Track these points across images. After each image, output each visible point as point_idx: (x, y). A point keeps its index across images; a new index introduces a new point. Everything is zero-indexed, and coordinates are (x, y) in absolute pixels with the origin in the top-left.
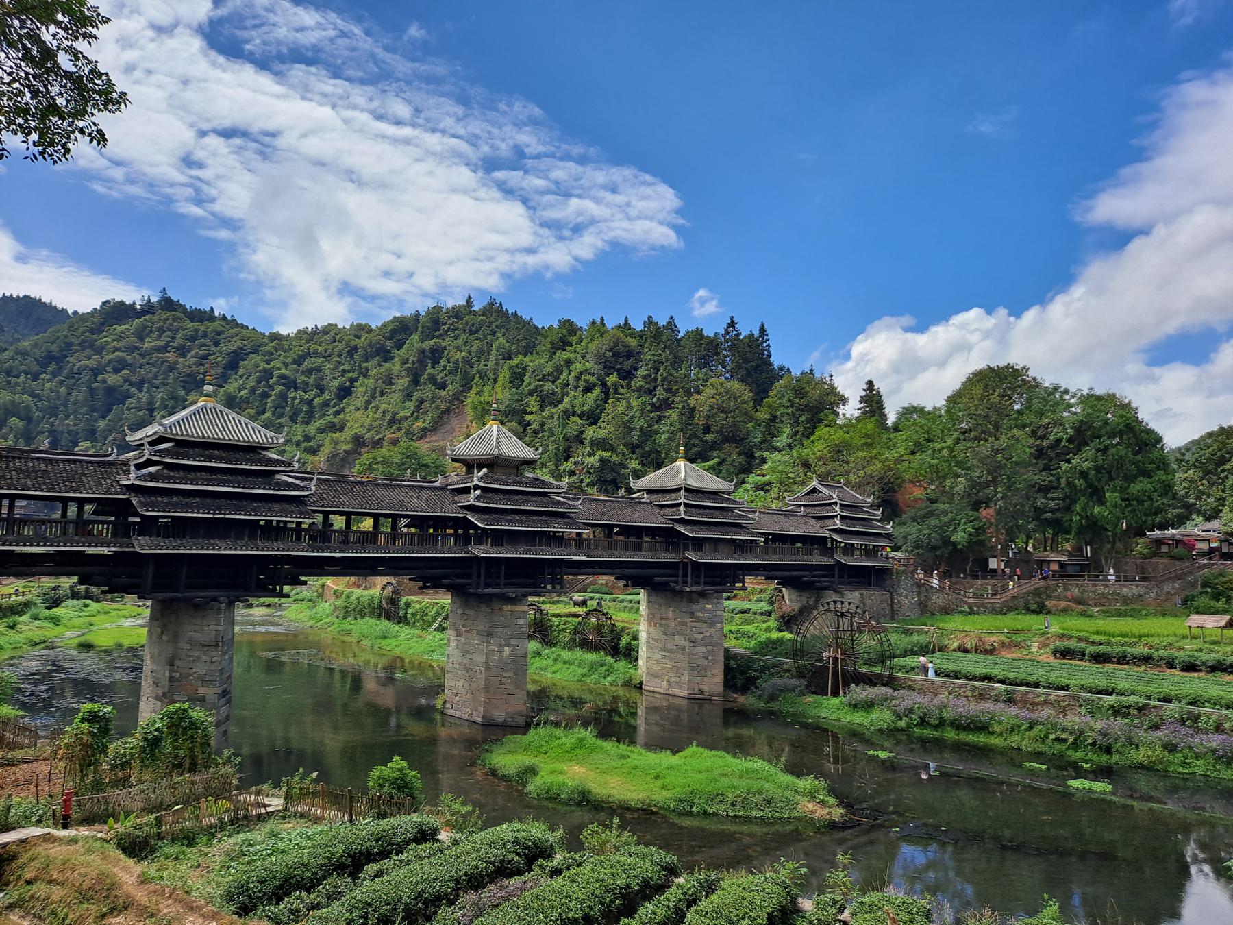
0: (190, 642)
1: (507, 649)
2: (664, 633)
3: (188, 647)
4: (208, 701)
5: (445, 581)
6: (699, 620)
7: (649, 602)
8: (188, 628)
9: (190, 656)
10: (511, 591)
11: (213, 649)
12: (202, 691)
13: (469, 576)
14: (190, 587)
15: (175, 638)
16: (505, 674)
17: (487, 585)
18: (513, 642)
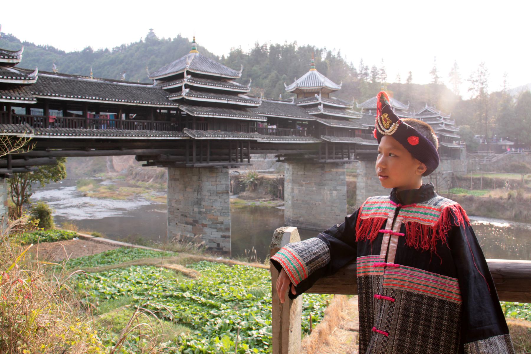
0: (209, 191)
1: (335, 192)
3: (208, 194)
4: (224, 224)
7: (366, 167)
8: (207, 183)
9: (211, 199)
11: (225, 195)
12: (221, 219)
14: (212, 160)
18: (338, 188)
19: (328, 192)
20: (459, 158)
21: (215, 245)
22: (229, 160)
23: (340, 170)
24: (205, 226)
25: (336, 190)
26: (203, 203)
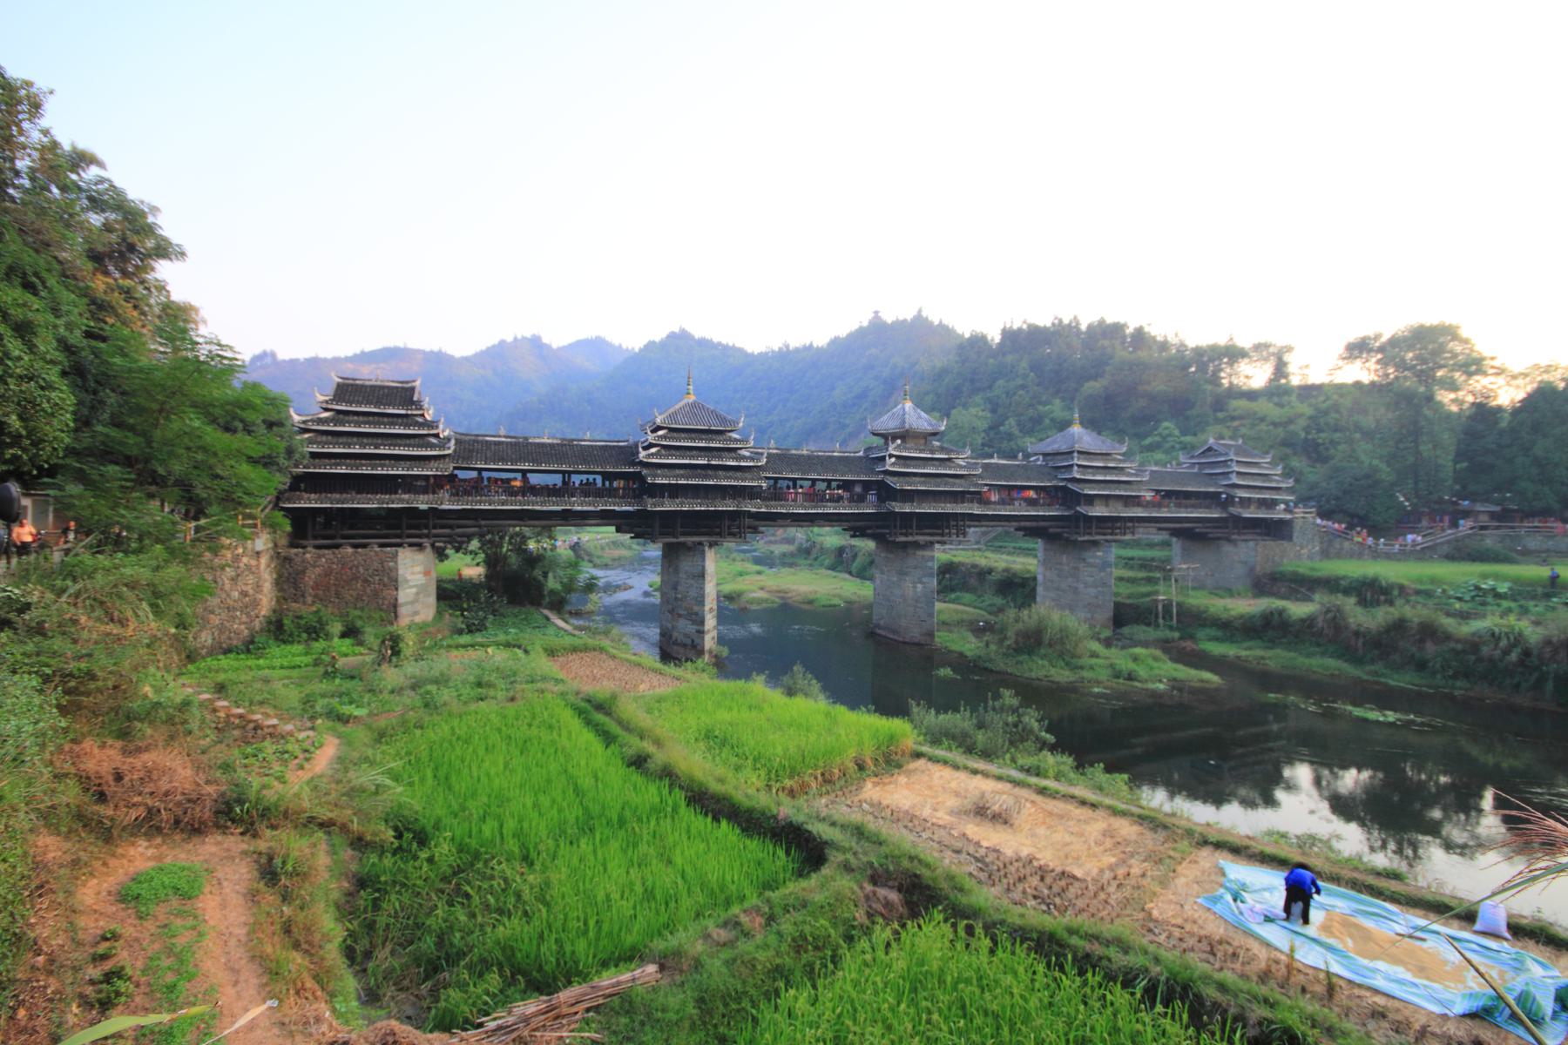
2: (1059, 576)
5: (869, 531)
6: (1092, 565)
7: (1045, 549)
10: (921, 539)
13: (887, 527)
14: (684, 534)
15: (676, 571)
17: (906, 535)
20: (1289, 538)
21: (689, 641)
22: (720, 534)
23: (927, 553)
24: (680, 616)
25: (921, 582)
26: (680, 588)
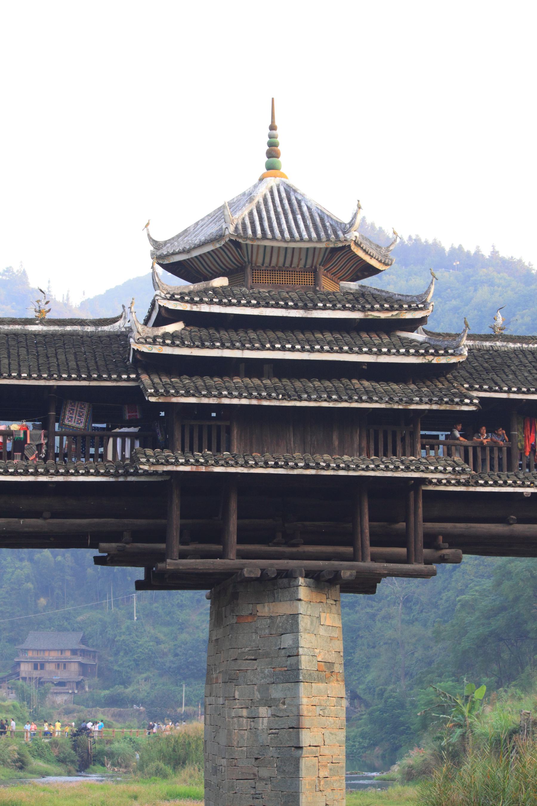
1: (263, 711)
16: (264, 773)
19: (245, 713)
25: (268, 703)
